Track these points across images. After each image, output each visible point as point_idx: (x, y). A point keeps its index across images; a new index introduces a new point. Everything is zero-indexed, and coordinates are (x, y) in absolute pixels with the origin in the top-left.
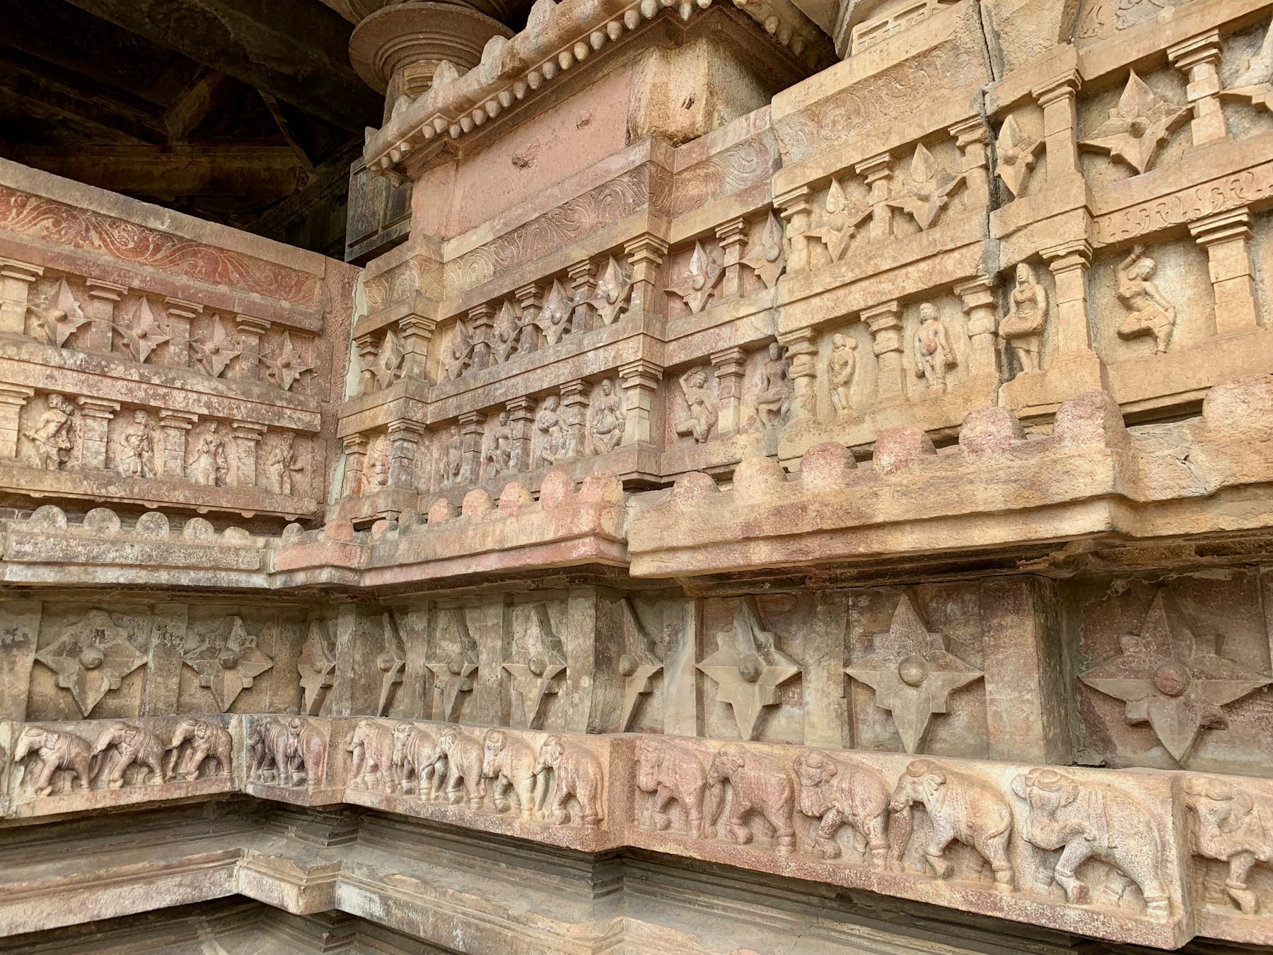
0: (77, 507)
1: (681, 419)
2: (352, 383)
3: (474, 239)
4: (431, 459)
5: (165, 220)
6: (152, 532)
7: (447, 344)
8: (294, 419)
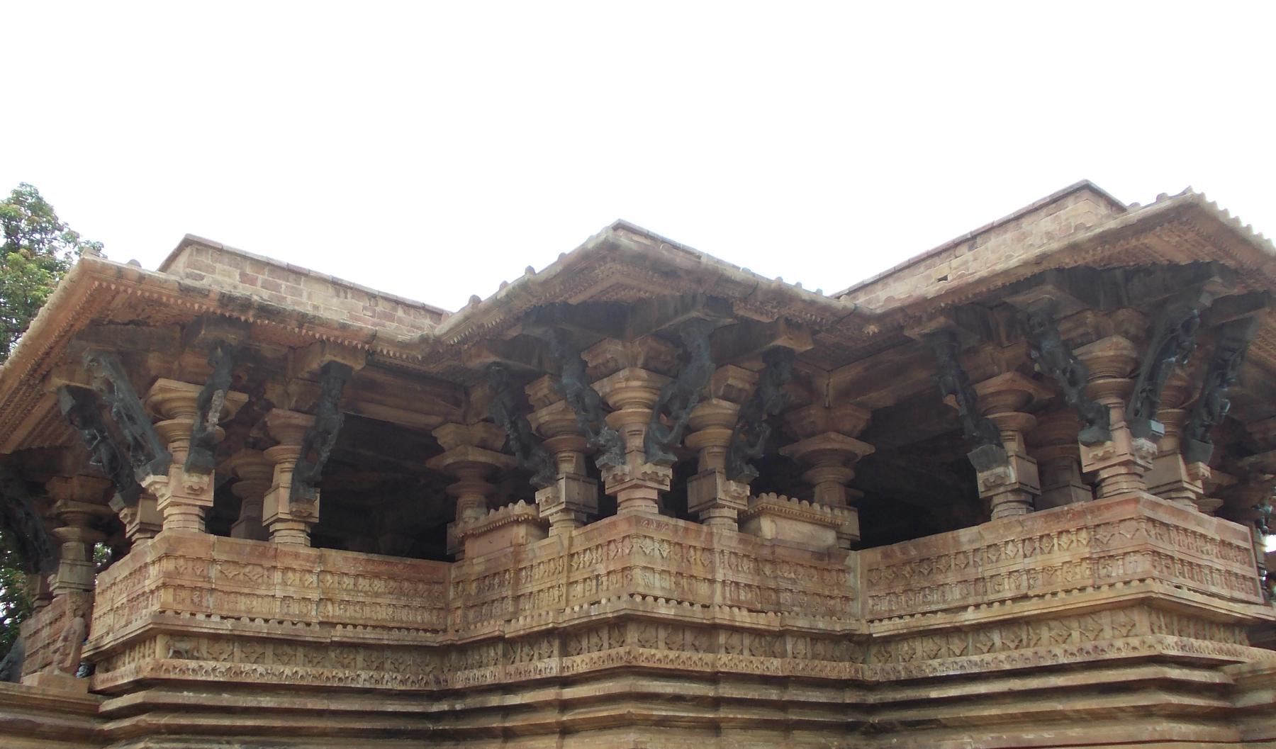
0: (399, 629)
1: (521, 606)
2: (452, 595)
3: (480, 560)
4: (471, 614)
5: (409, 561)
6: (413, 633)
7: (474, 585)
8: (439, 605)
